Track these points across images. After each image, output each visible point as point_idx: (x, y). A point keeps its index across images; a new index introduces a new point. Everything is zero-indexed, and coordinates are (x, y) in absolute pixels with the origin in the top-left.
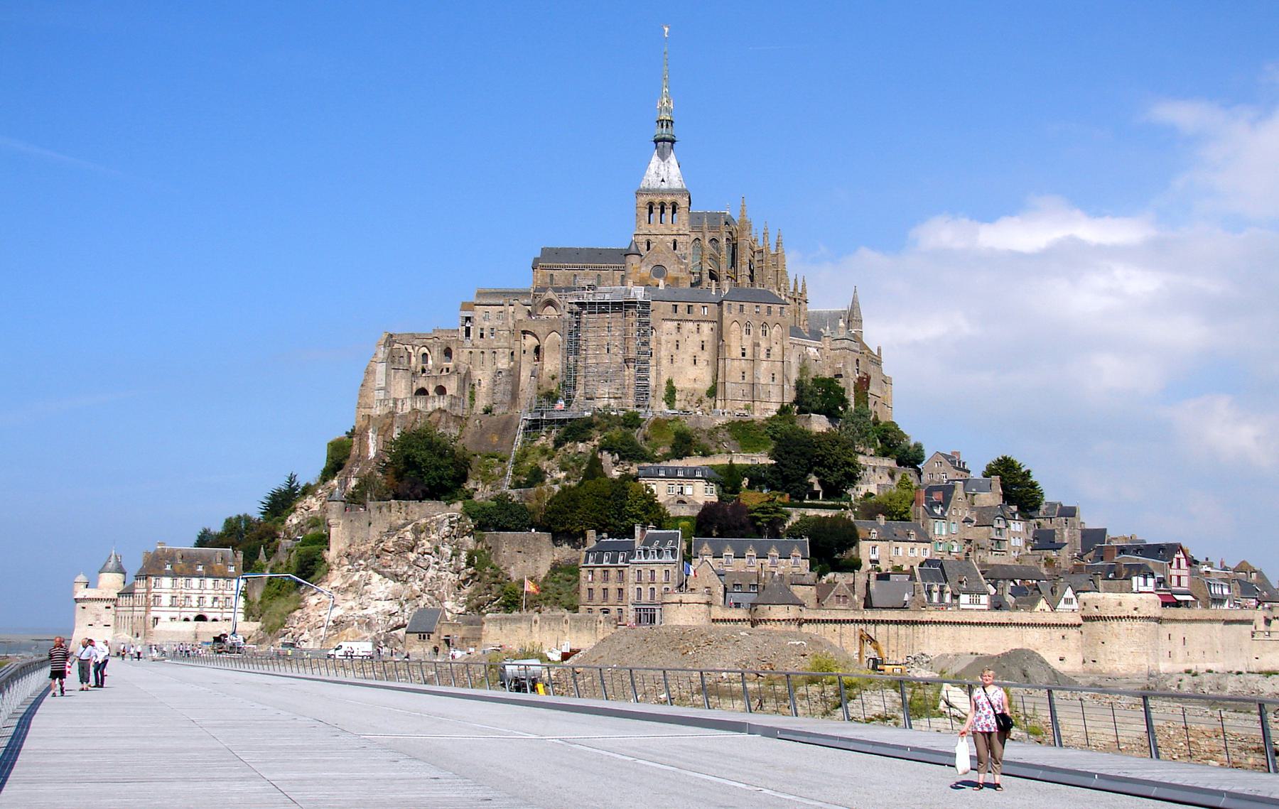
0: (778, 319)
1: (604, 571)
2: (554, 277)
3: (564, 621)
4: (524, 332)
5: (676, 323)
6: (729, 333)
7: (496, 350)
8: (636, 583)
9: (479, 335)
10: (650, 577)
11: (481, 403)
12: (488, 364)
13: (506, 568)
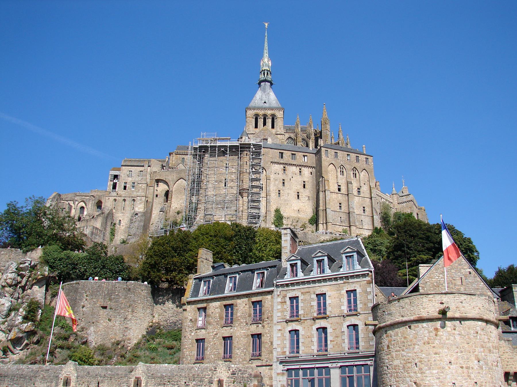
0: (365, 166)
1: (225, 306)
2: (185, 160)
3: (133, 380)
4: (158, 181)
5: (282, 166)
6: (327, 172)
7: (135, 198)
8: (287, 322)
9: (123, 187)
10: (316, 308)
11: (119, 237)
12: (128, 208)
13: (83, 329)
